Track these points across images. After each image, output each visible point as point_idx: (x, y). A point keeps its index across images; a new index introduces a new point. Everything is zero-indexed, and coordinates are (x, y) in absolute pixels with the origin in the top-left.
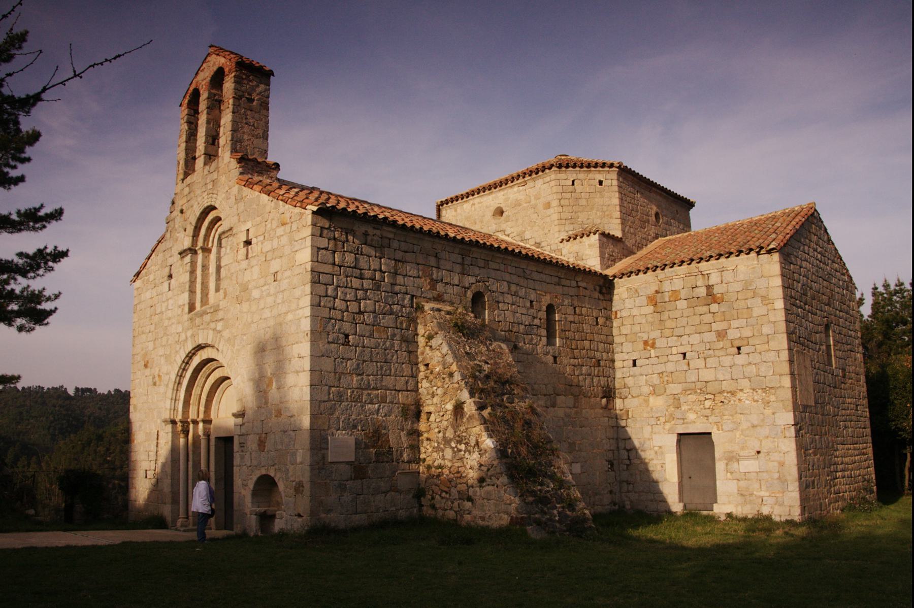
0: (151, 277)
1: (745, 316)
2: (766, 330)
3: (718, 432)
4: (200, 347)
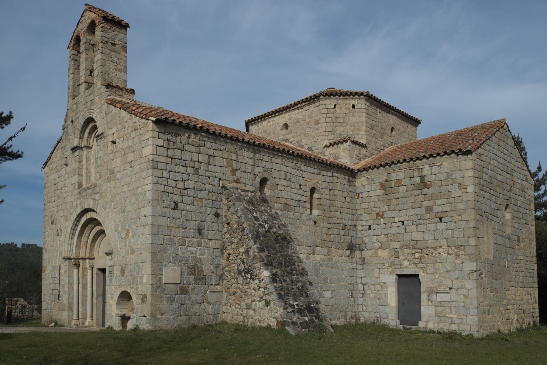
0: (54, 165)
1: (446, 197)
2: (460, 206)
3: (423, 274)
4: (86, 211)
